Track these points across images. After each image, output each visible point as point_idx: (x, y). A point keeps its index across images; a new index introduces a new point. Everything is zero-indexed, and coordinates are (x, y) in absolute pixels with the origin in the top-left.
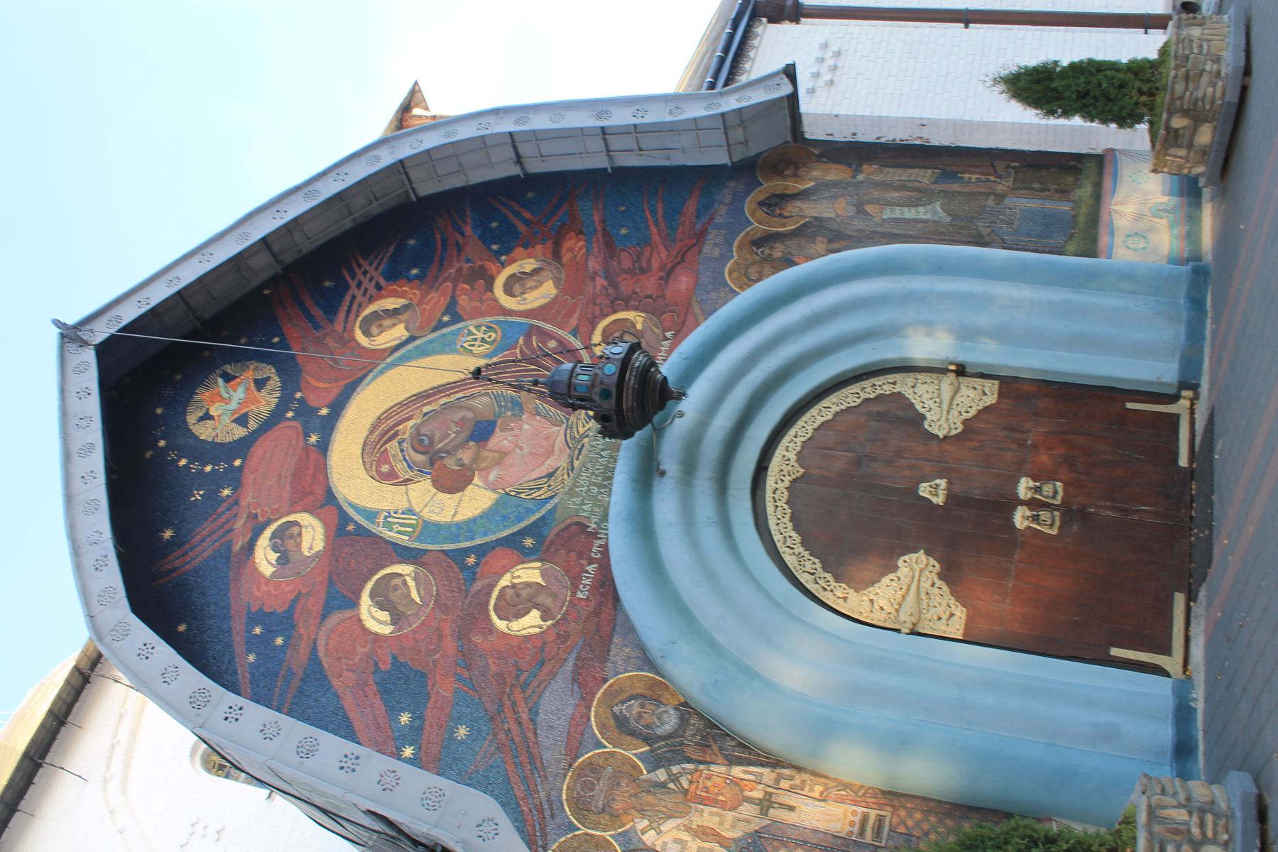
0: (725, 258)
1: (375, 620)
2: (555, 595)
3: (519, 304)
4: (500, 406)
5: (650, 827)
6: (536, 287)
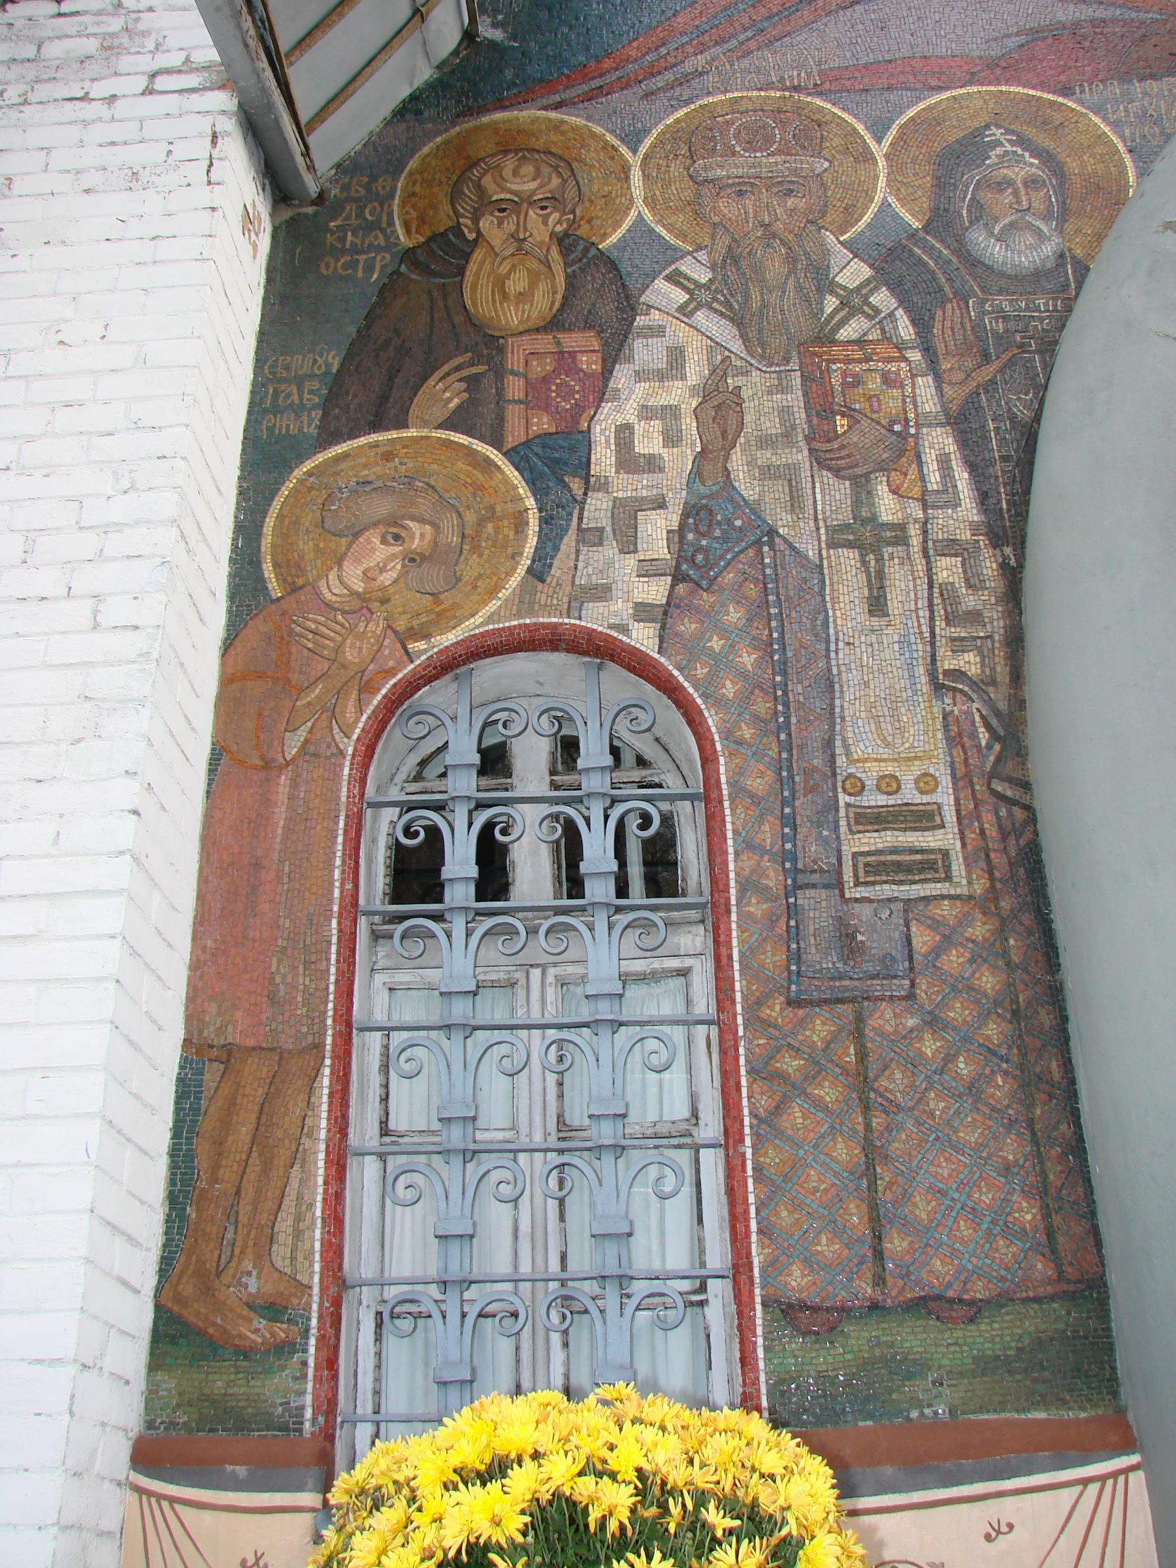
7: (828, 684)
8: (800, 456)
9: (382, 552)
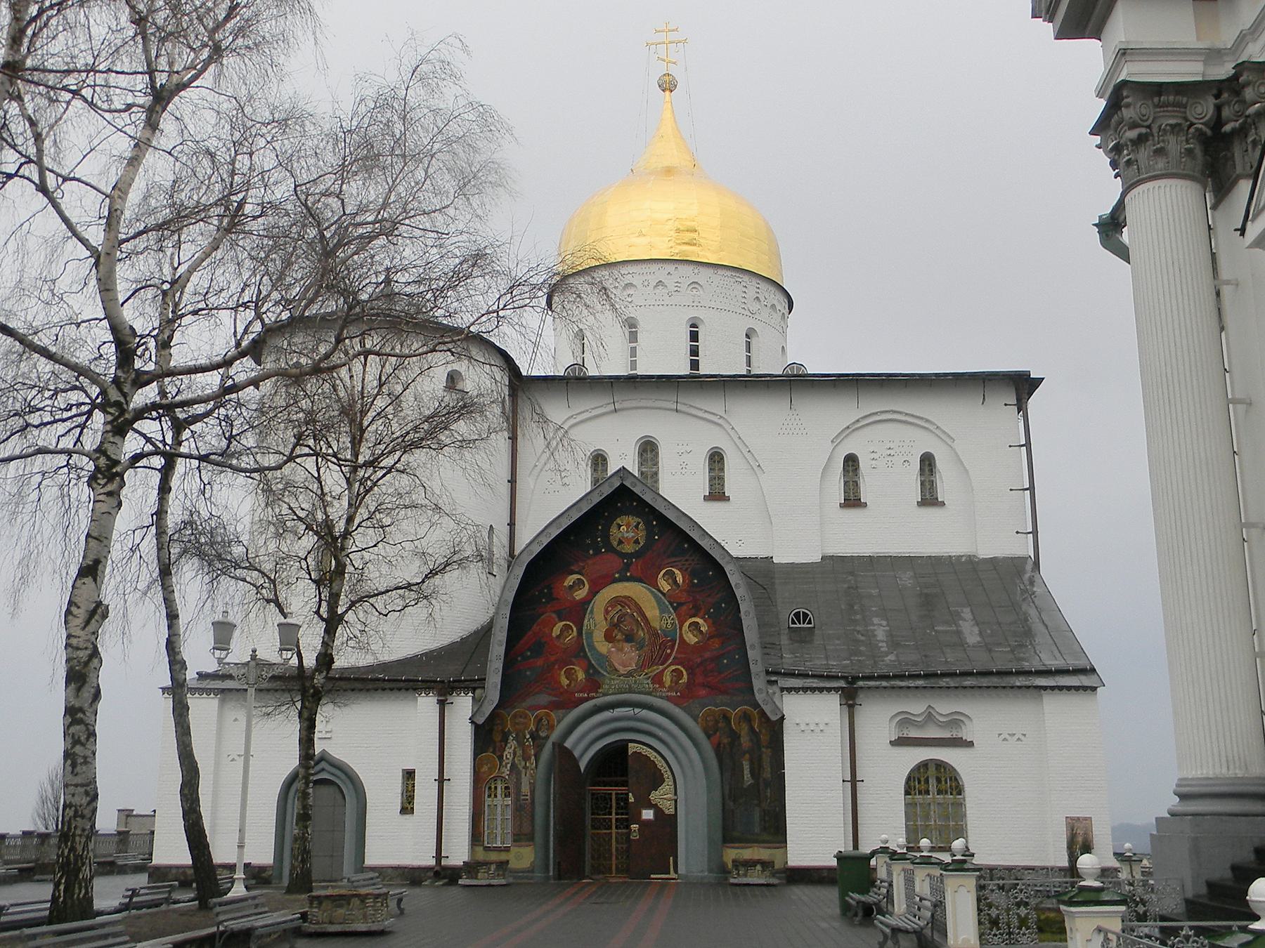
1: (556, 631)
2: (575, 686)
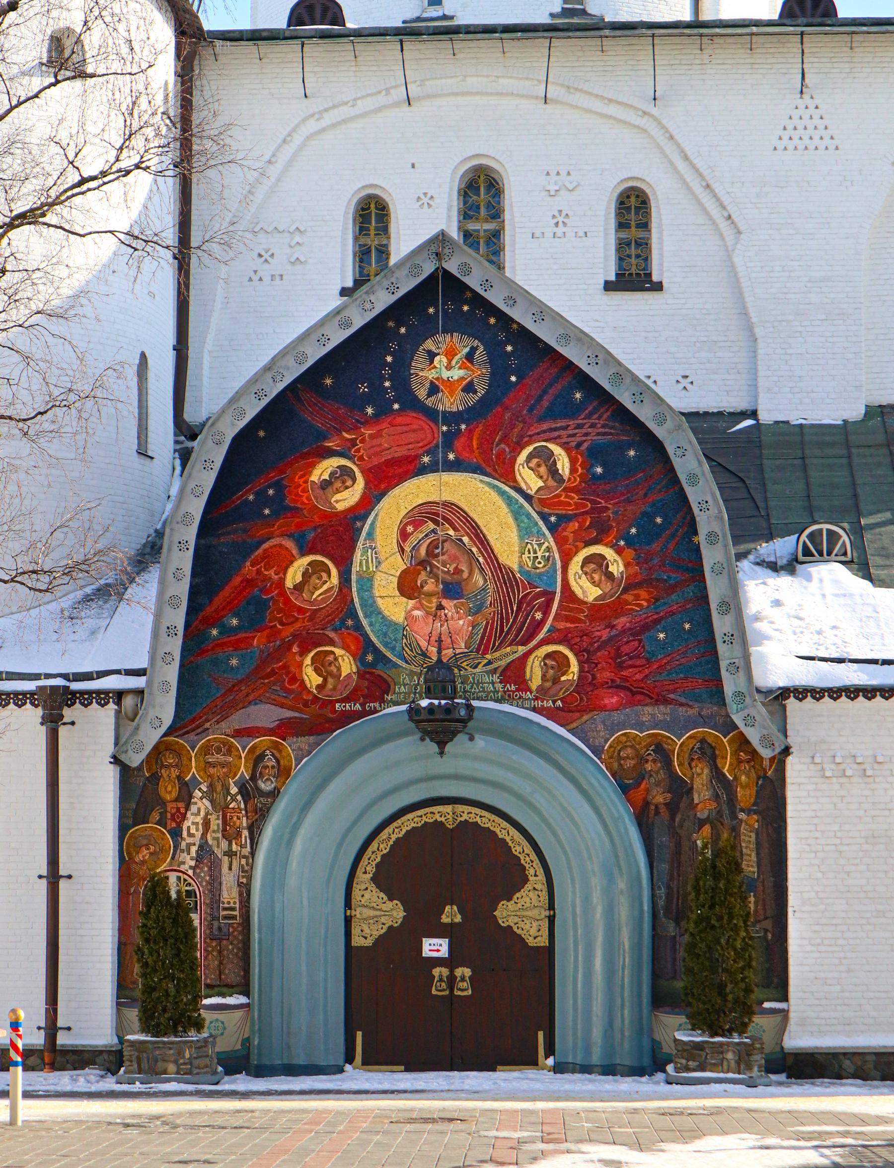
0: (640, 726)
2: (334, 689)
3: (575, 575)
4: (476, 595)
5: (203, 792)
6: (593, 583)
7: (220, 884)
8: (220, 835)
9: (146, 852)
